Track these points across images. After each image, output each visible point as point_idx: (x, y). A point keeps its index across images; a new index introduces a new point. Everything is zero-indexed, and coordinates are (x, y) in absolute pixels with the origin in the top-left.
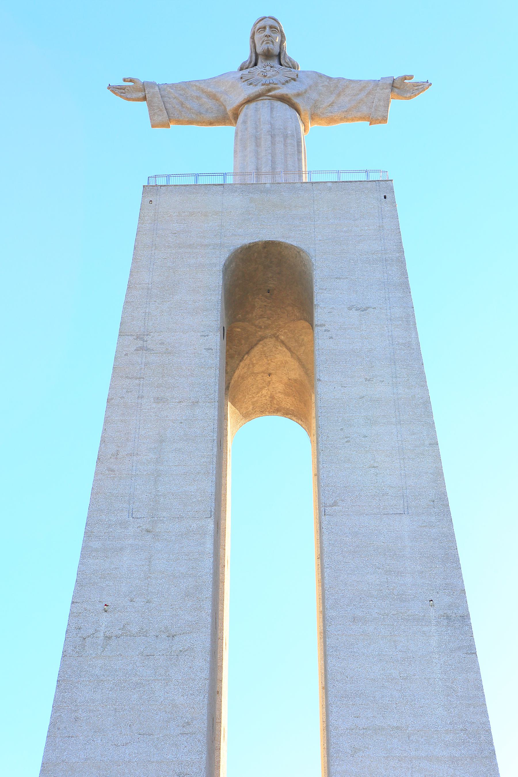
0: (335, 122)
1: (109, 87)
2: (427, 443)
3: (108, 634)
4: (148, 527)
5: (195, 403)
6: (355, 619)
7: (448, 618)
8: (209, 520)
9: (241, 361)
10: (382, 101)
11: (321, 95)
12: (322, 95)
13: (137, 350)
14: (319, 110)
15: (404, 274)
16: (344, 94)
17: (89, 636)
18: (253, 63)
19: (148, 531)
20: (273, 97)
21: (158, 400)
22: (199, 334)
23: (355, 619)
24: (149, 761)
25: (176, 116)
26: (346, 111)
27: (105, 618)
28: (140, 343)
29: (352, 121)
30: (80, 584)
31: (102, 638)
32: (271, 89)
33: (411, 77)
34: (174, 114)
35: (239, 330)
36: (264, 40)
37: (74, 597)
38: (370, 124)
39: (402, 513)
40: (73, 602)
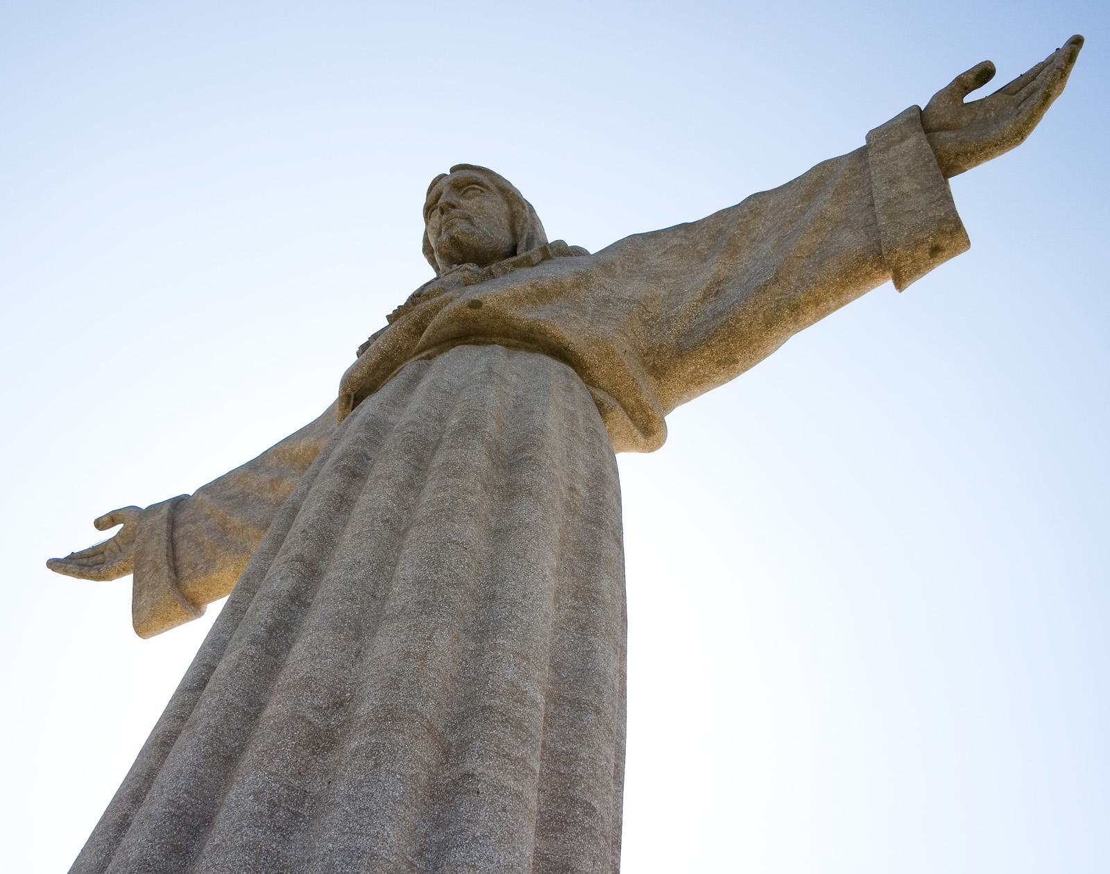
0: (751, 343)
1: (54, 564)
10: (904, 181)
11: (664, 280)
12: (669, 277)
14: (669, 329)
16: (754, 240)
20: (436, 345)
25: (202, 568)
26: (776, 280)
29: (817, 305)
32: (421, 318)
33: (984, 73)
34: (197, 565)
36: (440, 225)
38: (900, 284)
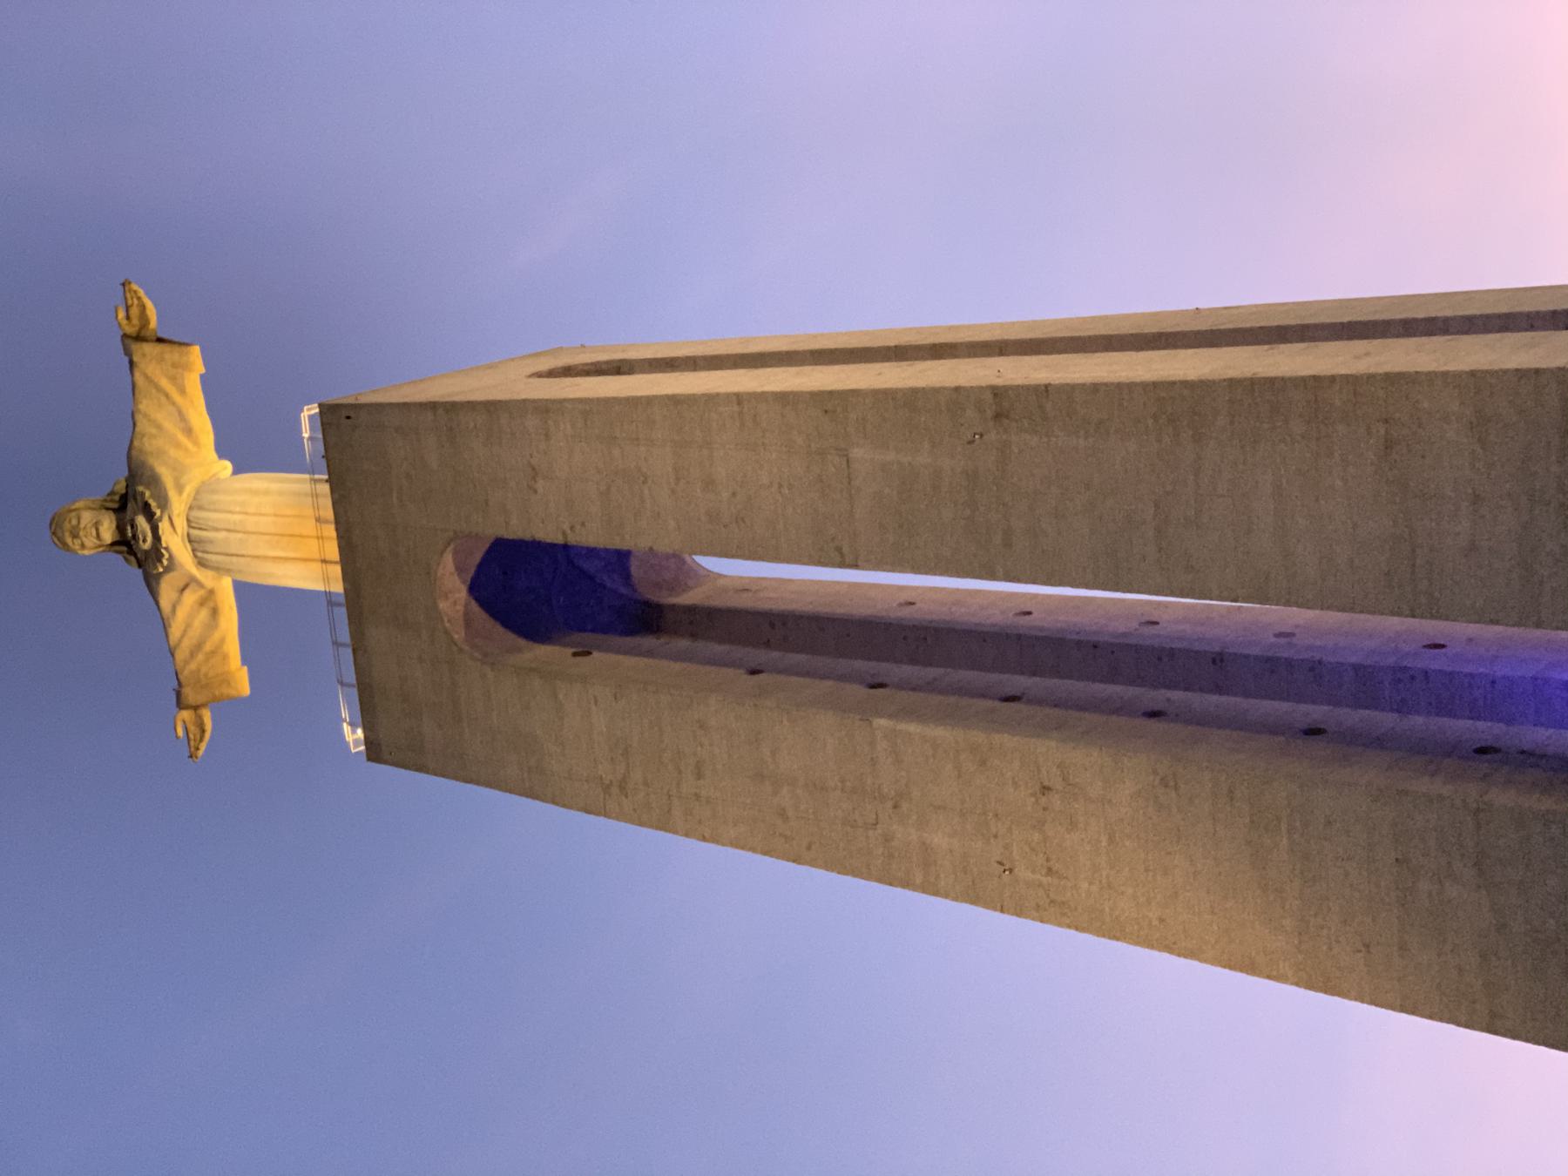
2: (736, 408)
3: (1044, 872)
4: (890, 804)
5: (702, 725)
6: (1007, 544)
7: (998, 416)
8: (874, 723)
9: (605, 587)
13: (626, 797)
15: (471, 406)
17: (1048, 896)
18: (125, 549)
19: (895, 807)
21: (699, 775)
22: (594, 707)
23: (1007, 544)
24: (1214, 834)
27: (1023, 873)
28: (615, 790)
30: (975, 900)
31: (1049, 878)
35: (562, 599)
37: (995, 909)
39: (845, 458)
40: (1002, 911)
